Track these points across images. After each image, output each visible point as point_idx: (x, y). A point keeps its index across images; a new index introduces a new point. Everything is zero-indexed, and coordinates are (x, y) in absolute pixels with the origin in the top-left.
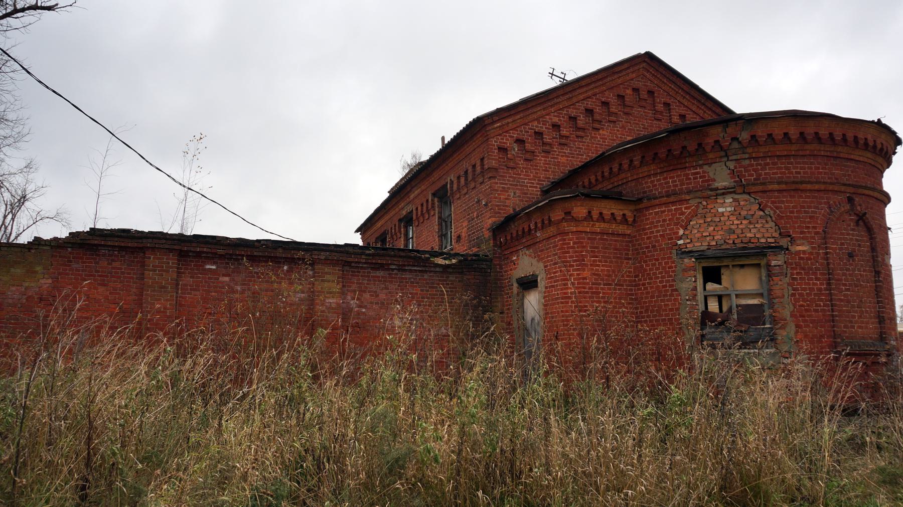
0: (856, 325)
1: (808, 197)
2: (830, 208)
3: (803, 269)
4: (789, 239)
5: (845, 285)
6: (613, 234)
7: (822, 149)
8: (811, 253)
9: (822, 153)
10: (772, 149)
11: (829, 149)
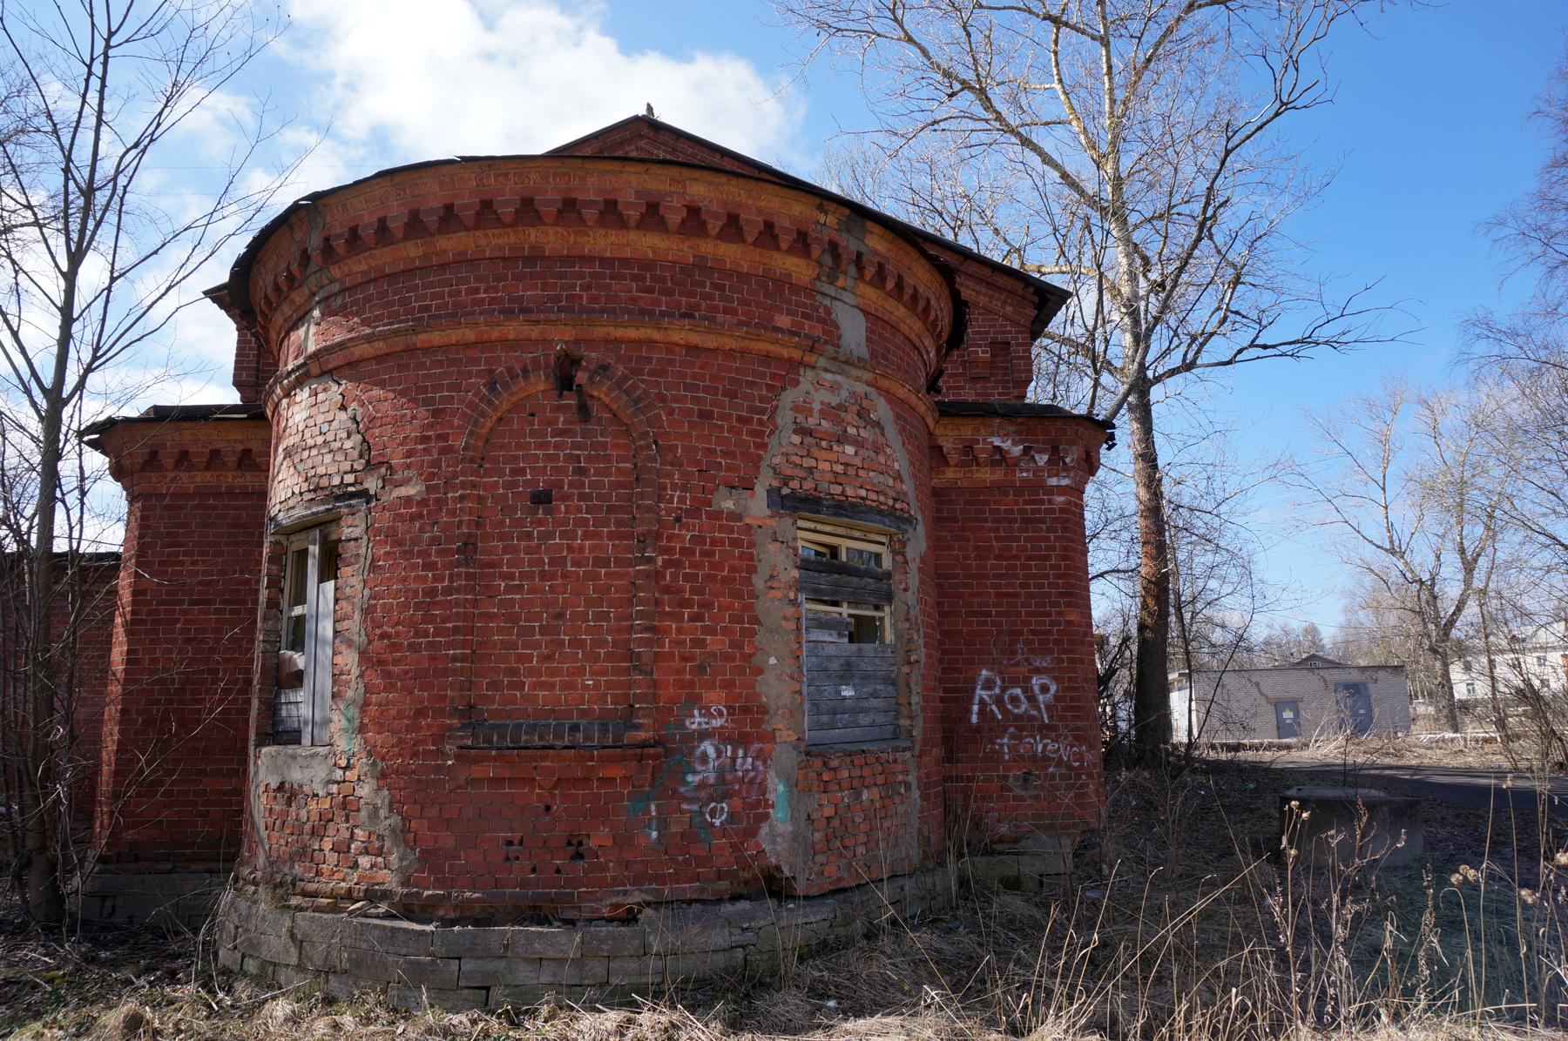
0: (528, 681)
1: (440, 364)
2: (491, 386)
5: (504, 577)
6: (231, 493)
8: (423, 502)
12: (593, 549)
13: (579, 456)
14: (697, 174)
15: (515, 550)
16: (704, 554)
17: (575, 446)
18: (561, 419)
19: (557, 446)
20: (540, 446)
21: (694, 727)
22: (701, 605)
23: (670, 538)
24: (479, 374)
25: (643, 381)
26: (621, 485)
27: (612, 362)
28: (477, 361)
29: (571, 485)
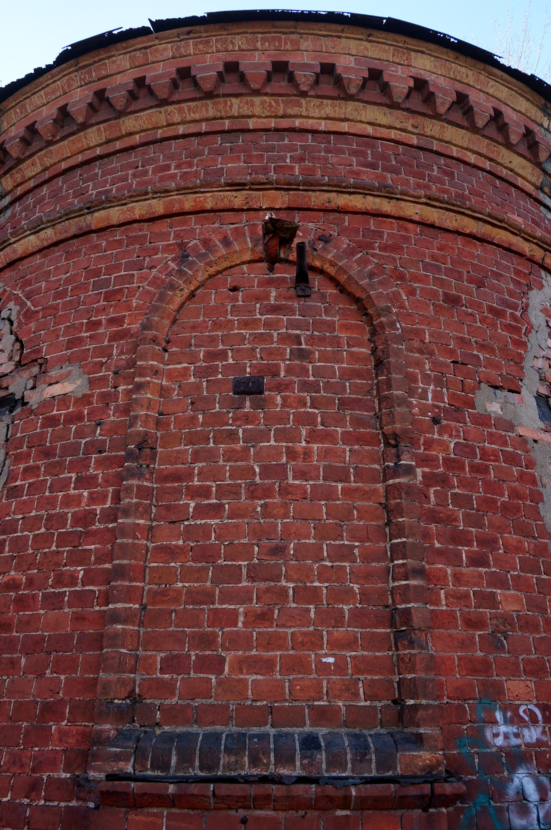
0: (229, 656)
2: (183, 258)
3: (48, 453)
4: (35, 370)
5: (194, 493)
7: (177, 118)
8: (86, 399)
9: (181, 130)
10: (48, 162)
11: (197, 116)
12: (325, 454)
13: (298, 337)
14: (423, 46)
15: (211, 455)
16: (475, 468)
17: (292, 325)
18: (273, 294)
19: (268, 325)
20: (246, 324)
21: (500, 741)
22: (482, 542)
23: (429, 444)
24: (167, 249)
25: (373, 255)
26: (358, 374)
27: (336, 234)
28: (165, 236)
29: (289, 370)
